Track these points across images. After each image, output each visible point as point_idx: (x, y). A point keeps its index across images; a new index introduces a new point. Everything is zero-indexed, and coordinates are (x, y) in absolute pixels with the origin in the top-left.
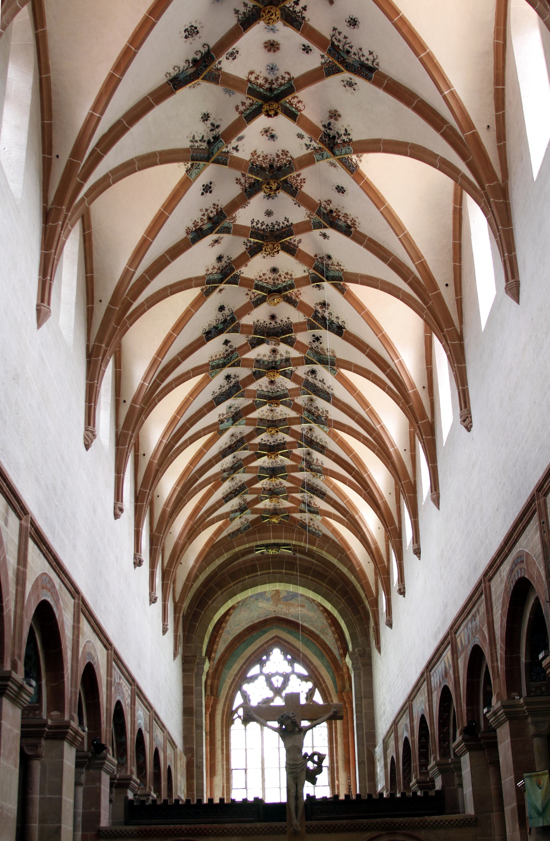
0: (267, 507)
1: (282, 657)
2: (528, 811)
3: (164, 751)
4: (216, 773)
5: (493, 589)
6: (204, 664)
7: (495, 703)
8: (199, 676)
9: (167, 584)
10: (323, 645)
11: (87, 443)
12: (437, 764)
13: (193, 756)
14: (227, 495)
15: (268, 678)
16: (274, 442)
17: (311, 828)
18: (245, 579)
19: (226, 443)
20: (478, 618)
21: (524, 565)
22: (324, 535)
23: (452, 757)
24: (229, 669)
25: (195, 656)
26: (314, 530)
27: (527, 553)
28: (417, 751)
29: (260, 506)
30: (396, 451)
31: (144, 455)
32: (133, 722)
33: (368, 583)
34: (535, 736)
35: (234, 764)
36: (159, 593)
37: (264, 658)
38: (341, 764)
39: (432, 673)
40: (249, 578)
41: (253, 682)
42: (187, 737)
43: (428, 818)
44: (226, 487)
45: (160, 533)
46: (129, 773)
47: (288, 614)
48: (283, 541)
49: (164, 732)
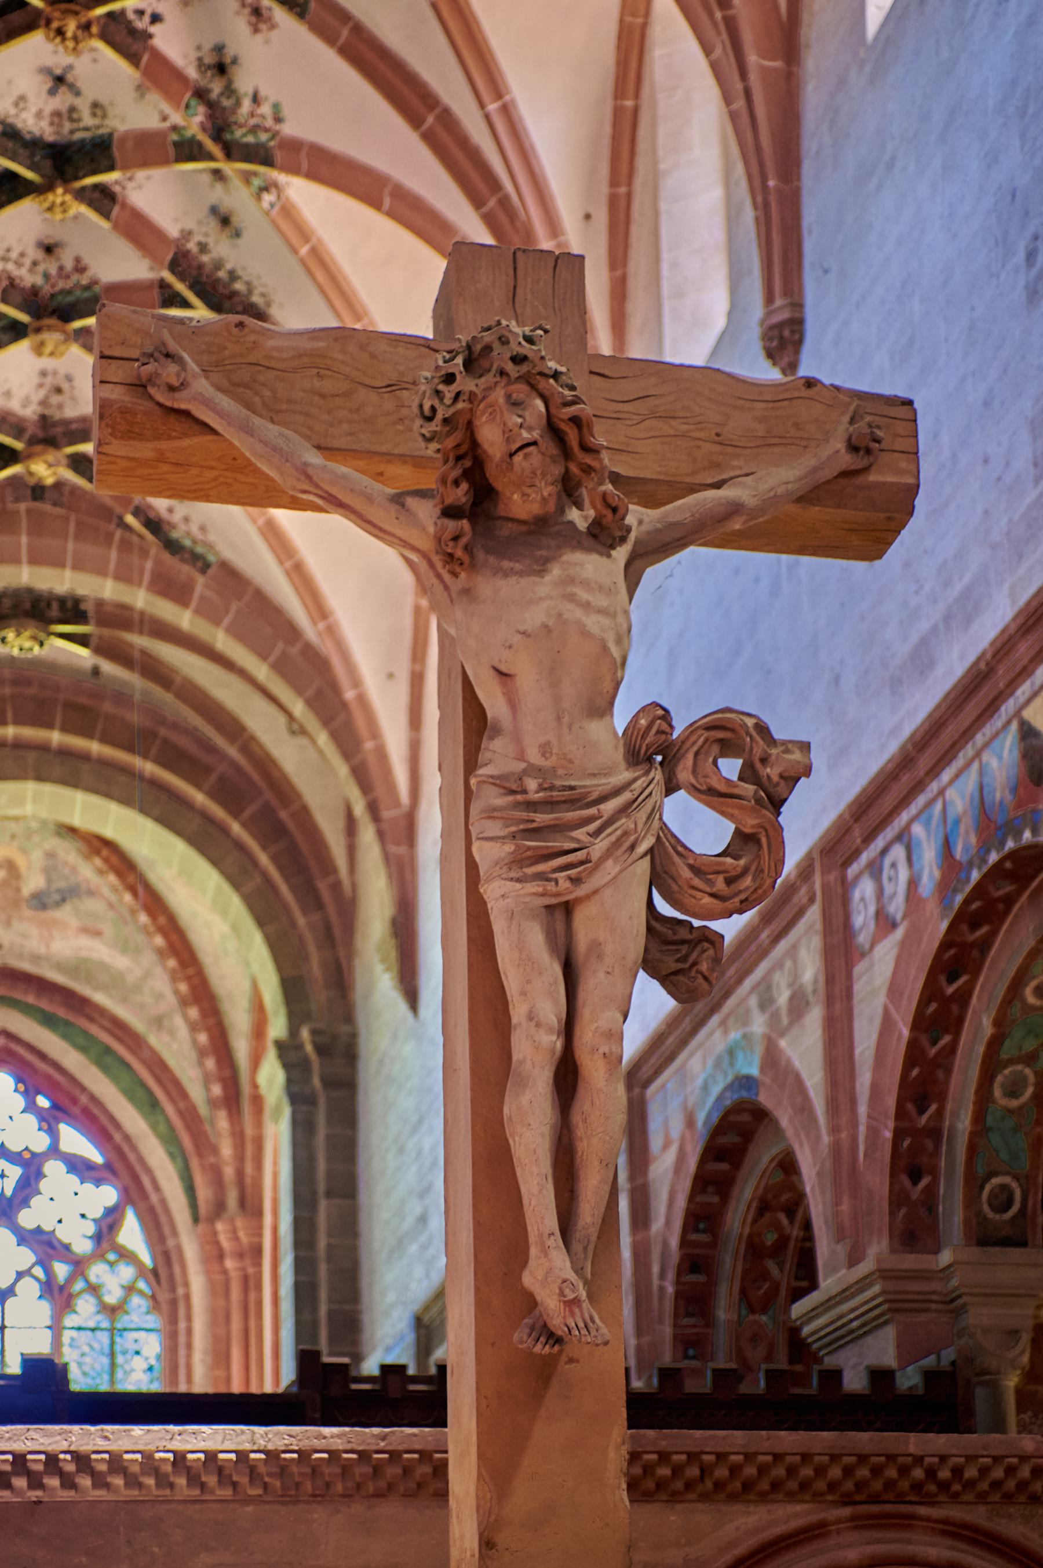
1: (20, 1102)
10: (159, 1067)
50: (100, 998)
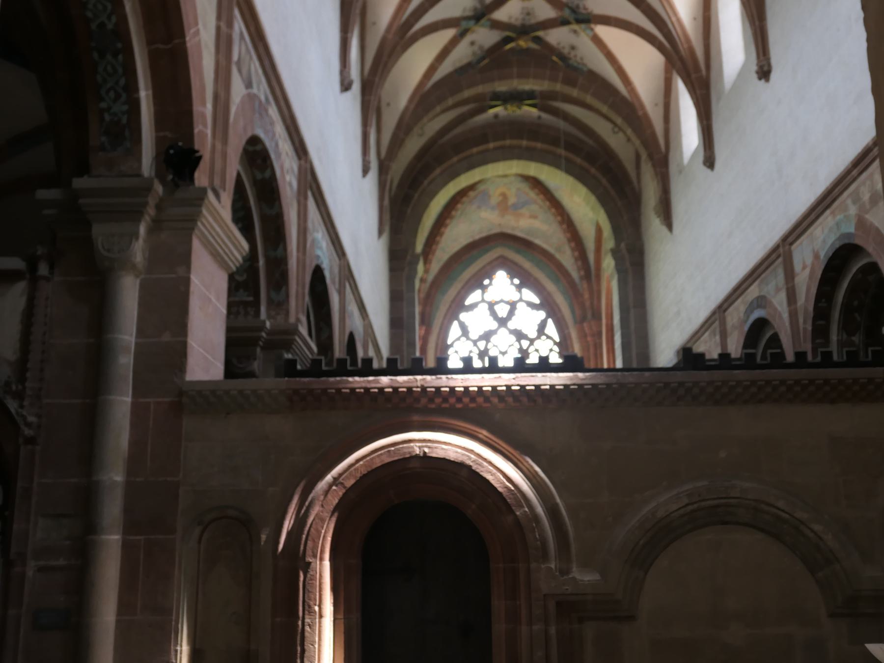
1: (509, 281)
15: (491, 306)
17: (783, 389)
26: (575, 64)
33: (654, 134)
36: (355, 73)
37: (486, 282)
46: (292, 320)
50: (537, 241)
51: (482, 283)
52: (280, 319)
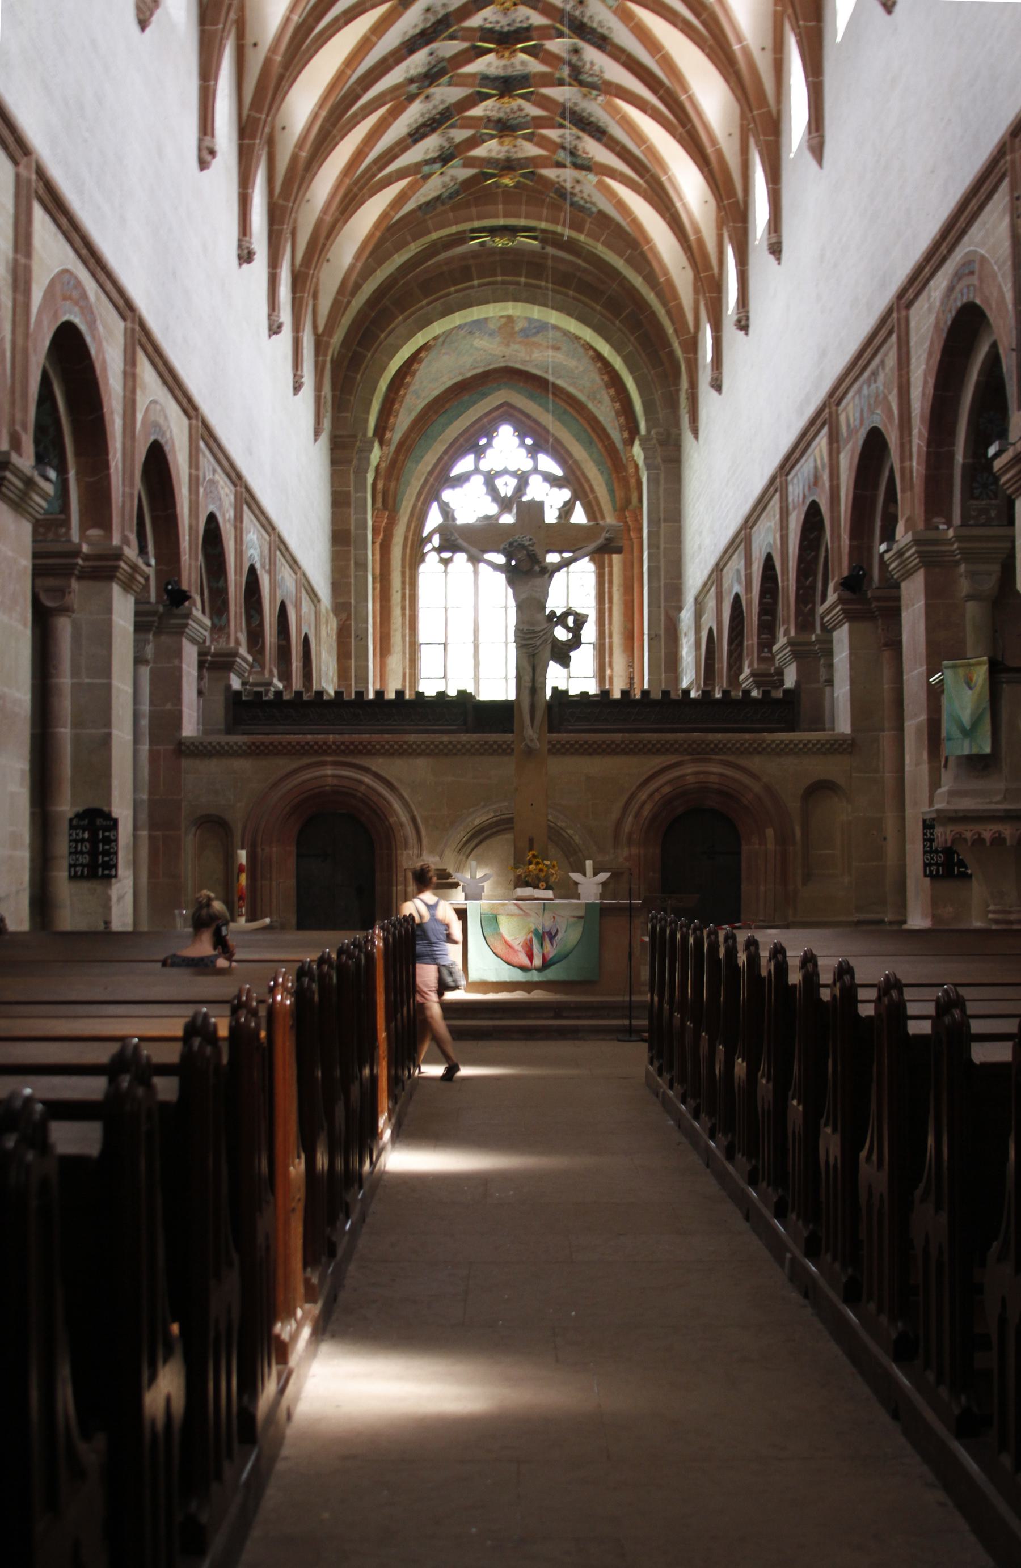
0: (494, 154)
1: (516, 441)
2: (947, 726)
3: (296, 606)
4: (392, 650)
5: (913, 324)
6: (370, 451)
7: (902, 535)
8: (361, 473)
9: (302, 298)
11: (141, 17)
12: (791, 643)
13: (349, 618)
14: (417, 129)
15: (490, 479)
16: (509, 25)
18: (449, 294)
19: (416, 26)
20: (881, 378)
21: (974, 280)
22: (601, 213)
23: (818, 631)
24: (417, 462)
25: (355, 436)
26: (582, 202)
27: (983, 258)
28: (755, 618)
29: (480, 152)
30: (746, 51)
31: (255, 45)
32: (239, 553)
33: (680, 307)
34: (970, 597)
35: (423, 636)
36: (285, 316)
37: (483, 441)
38: (617, 640)
39: (790, 477)
40: (456, 292)
41: (461, 486)
42: (339, 584)
43: (768, 737)
44: (414, 113)
45: (287, 199)
46: (232, 644)
47: (530, 361)
48: (522, 222)
49: (296, 574)
51: (477, 444)
52: (222, 642)
